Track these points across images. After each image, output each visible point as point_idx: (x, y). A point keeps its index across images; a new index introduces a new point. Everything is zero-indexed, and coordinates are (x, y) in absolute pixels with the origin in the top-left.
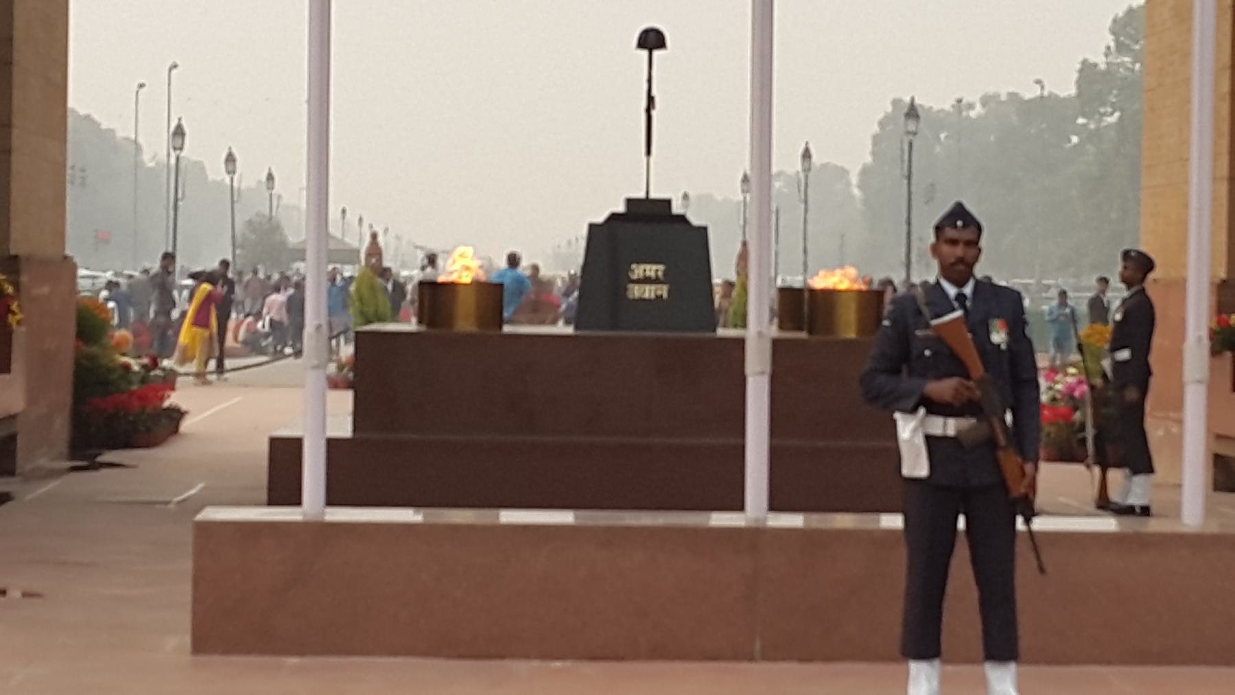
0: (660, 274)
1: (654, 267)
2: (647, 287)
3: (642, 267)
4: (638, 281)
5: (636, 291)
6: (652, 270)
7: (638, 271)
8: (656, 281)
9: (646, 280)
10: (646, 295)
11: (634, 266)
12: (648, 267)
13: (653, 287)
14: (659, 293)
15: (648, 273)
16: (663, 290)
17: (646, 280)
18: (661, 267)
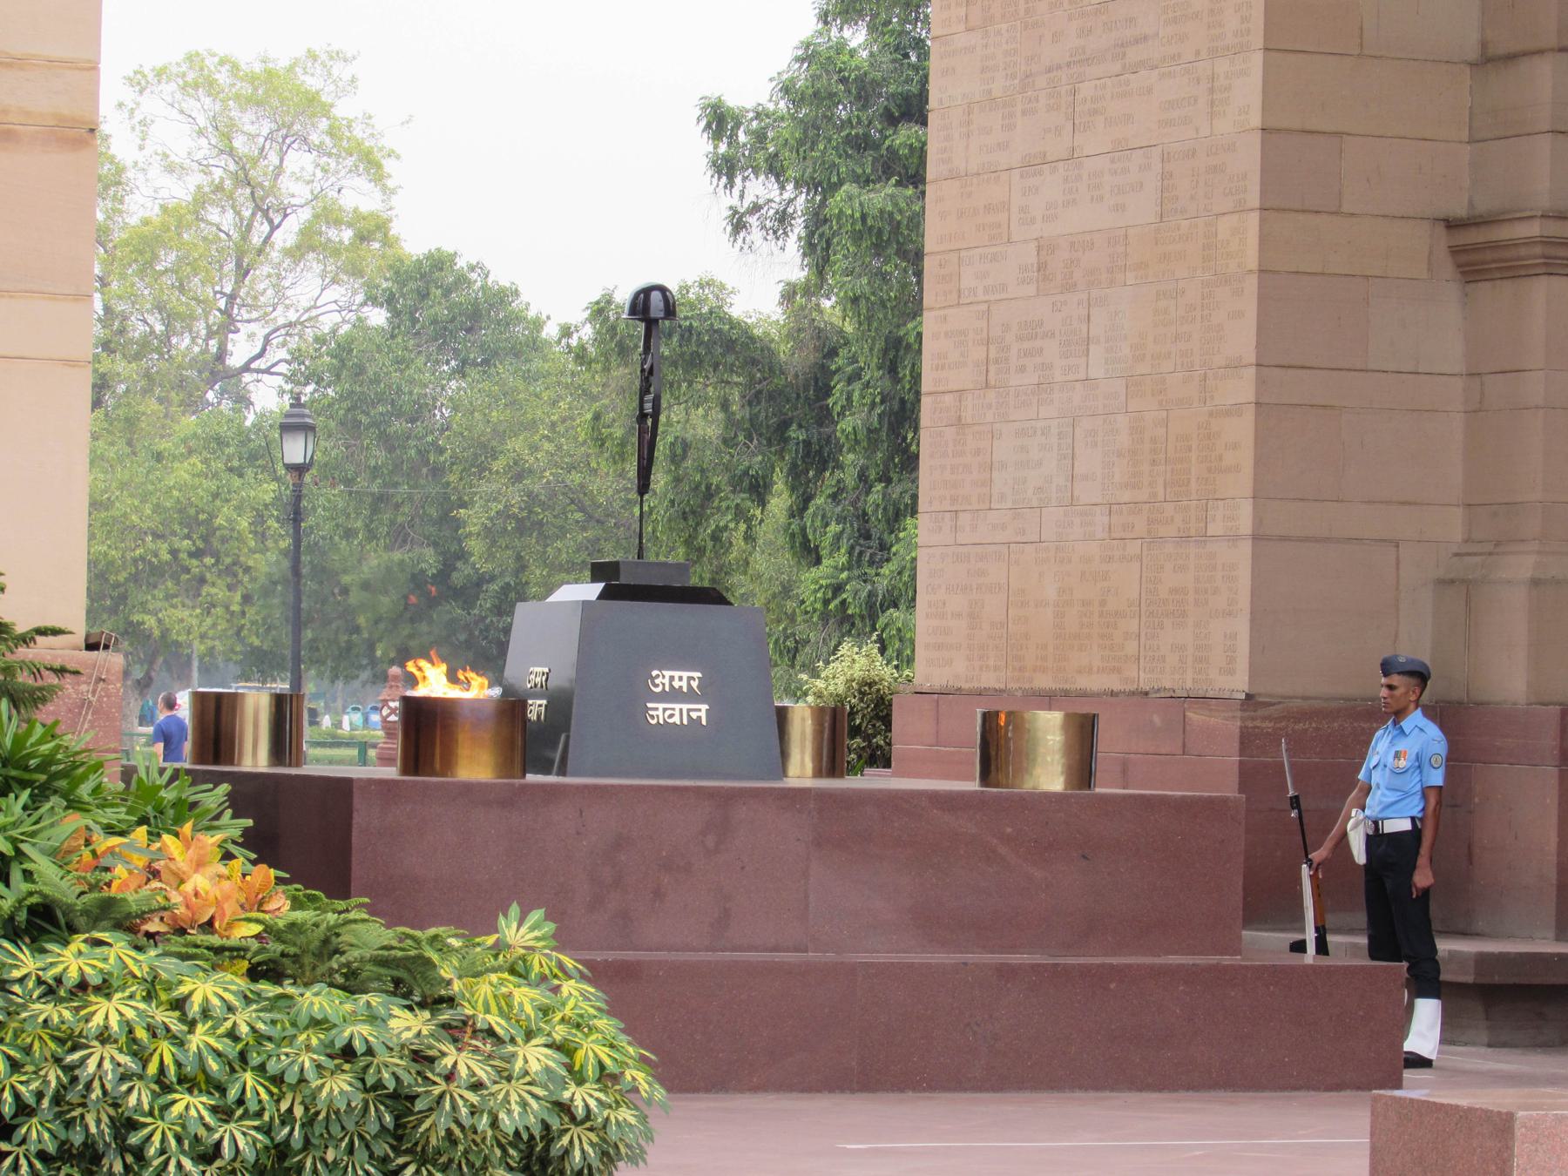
0: (695, 684)
1: (685, 675)
2: (677, 706)
3: (668, 673)
4: (665, 697)
5: (659, 712)
6: (684, 678)
7: (664, 678)
8: (689, 696)
9: (674, 695)
10: (676, 719)
11: (654, 673)
12: (677, 674)
13: (685, 707)
14: (694, 715)
15: (676, 684)
16: (701, 711)
17: (674, 695)
18: (697, 675)
